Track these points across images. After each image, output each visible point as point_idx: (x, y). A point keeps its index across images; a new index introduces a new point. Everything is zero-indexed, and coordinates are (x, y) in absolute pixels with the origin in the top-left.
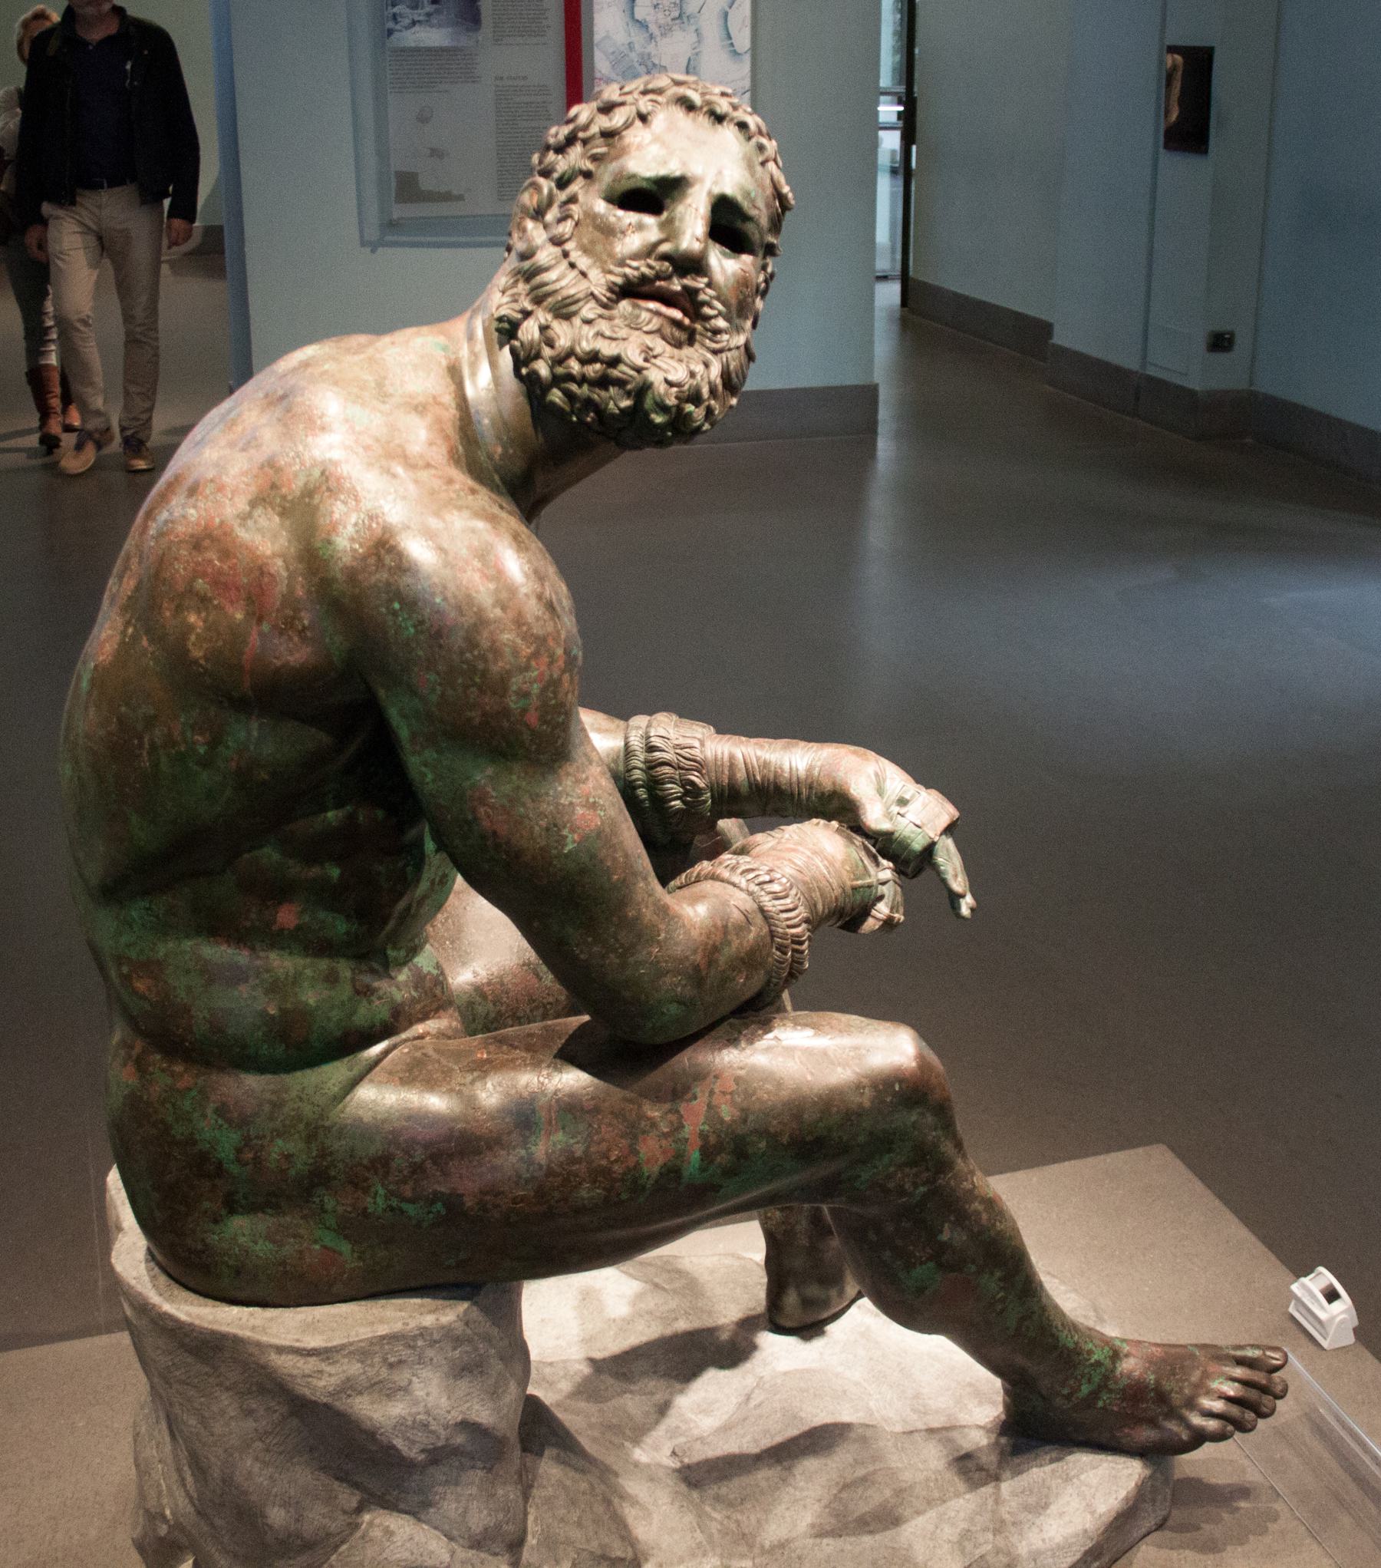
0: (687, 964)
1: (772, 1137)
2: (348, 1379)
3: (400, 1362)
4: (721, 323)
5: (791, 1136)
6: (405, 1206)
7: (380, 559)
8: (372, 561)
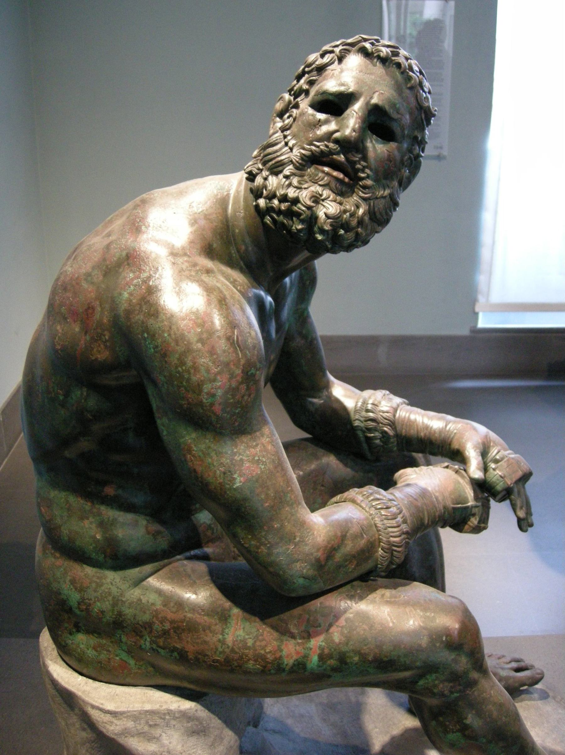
1: (363, 656)
2: (126, 729)
3: (156, 725)
4: (369, 182)
5: (374, 657)
6: (160, 650)
7: (141, 307)
8: (137, 308)
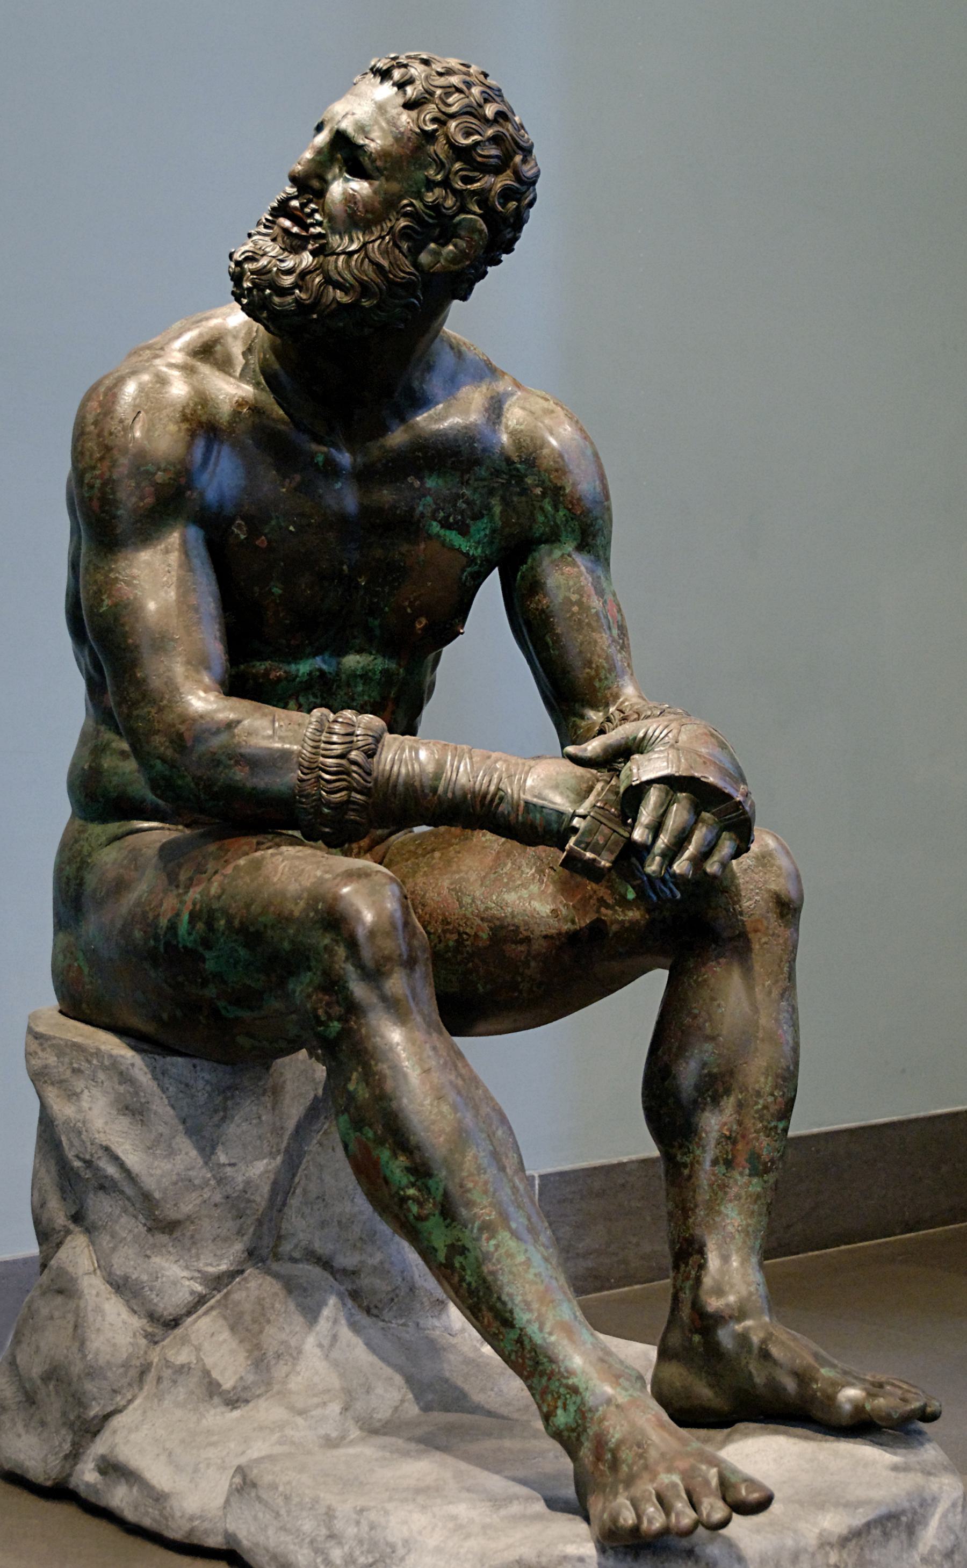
0: (173, 730)
